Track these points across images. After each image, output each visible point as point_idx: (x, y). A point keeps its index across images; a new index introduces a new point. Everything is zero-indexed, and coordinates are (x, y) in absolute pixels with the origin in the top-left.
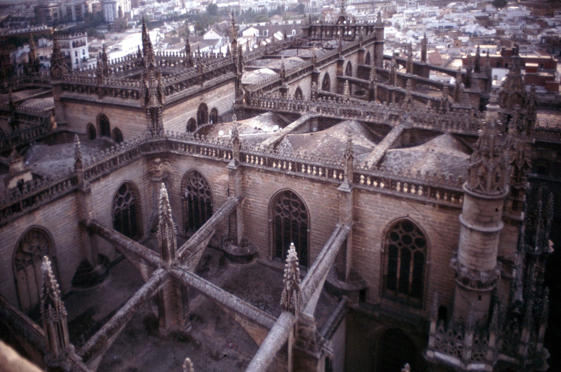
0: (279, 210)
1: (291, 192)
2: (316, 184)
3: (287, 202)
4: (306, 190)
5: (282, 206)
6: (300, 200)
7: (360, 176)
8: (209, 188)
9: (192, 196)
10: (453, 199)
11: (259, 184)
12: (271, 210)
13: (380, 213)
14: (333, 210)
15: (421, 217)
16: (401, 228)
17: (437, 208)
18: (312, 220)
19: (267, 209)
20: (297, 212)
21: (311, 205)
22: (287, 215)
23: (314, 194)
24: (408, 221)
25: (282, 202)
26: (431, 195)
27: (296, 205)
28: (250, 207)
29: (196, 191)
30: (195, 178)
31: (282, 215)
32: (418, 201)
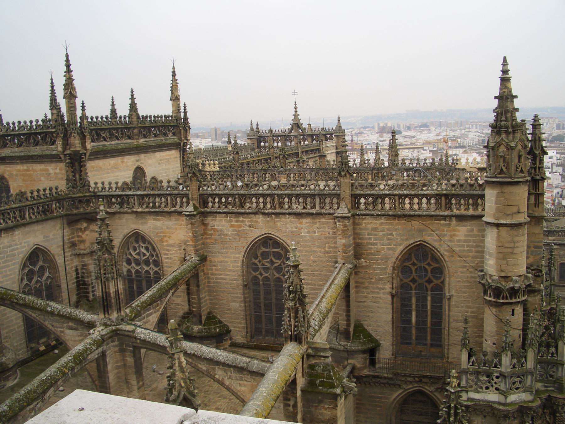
0: (256, 269)
2: (304, 221)
3: (265, 255)
5: (260, 262)
9: (133, 271)
13: (388, 241)
14: (328, 252)
16: (414, 260)
20: (280, 265)
22: (266, 273)
23: (302, 234)
25: (259, 255)
26: (446, 208)
28: (216, 270)
29: (138, 263)
30: (136, 245)
31: (261, 274)
32: (431, 216)
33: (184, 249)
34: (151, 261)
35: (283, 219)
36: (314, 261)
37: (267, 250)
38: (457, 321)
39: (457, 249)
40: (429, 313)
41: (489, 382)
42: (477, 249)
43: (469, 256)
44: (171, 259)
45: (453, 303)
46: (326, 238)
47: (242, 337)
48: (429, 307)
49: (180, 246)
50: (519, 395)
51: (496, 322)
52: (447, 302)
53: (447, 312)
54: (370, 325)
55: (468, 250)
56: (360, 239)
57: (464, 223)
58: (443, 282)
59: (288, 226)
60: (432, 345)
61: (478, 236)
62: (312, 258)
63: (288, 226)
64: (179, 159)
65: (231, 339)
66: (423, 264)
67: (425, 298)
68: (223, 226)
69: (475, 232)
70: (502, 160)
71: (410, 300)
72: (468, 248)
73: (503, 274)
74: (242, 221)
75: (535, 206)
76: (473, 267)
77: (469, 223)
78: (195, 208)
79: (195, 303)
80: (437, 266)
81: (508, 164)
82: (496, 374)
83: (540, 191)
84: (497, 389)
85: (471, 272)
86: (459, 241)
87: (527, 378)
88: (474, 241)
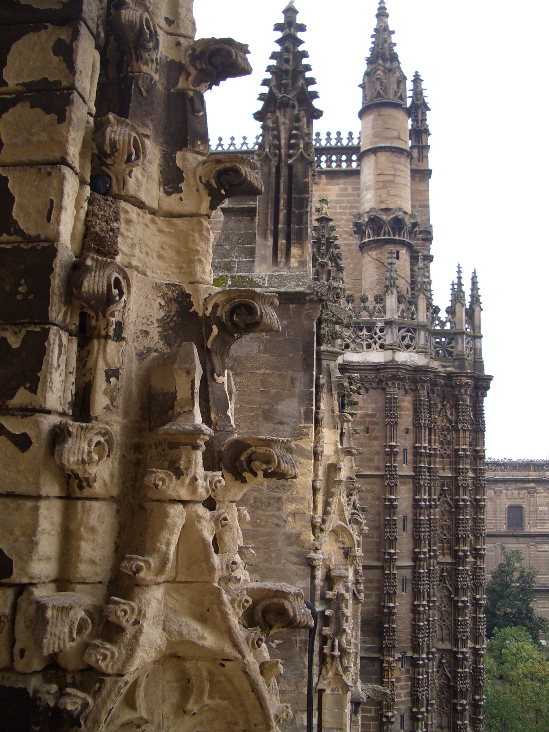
41: (372, 338)
42: (351, 211)
43: (342, 220)
50: (411, 354)
51: (377, 268)
55: (341, 213)
57: (335, 181)
61: (353, 195)
69: (350, 191)
70: (378, 83)
72: (341, 210)
73: (383, 206)
75: (419, 161)
76: (347, 232)
77: (341, 181)
81: (386, 88)
82: (380, 325)
83: (424, 144)
84: (382, 347)
85: (345, 239)
87: (419, 335)
88: (348, 202)
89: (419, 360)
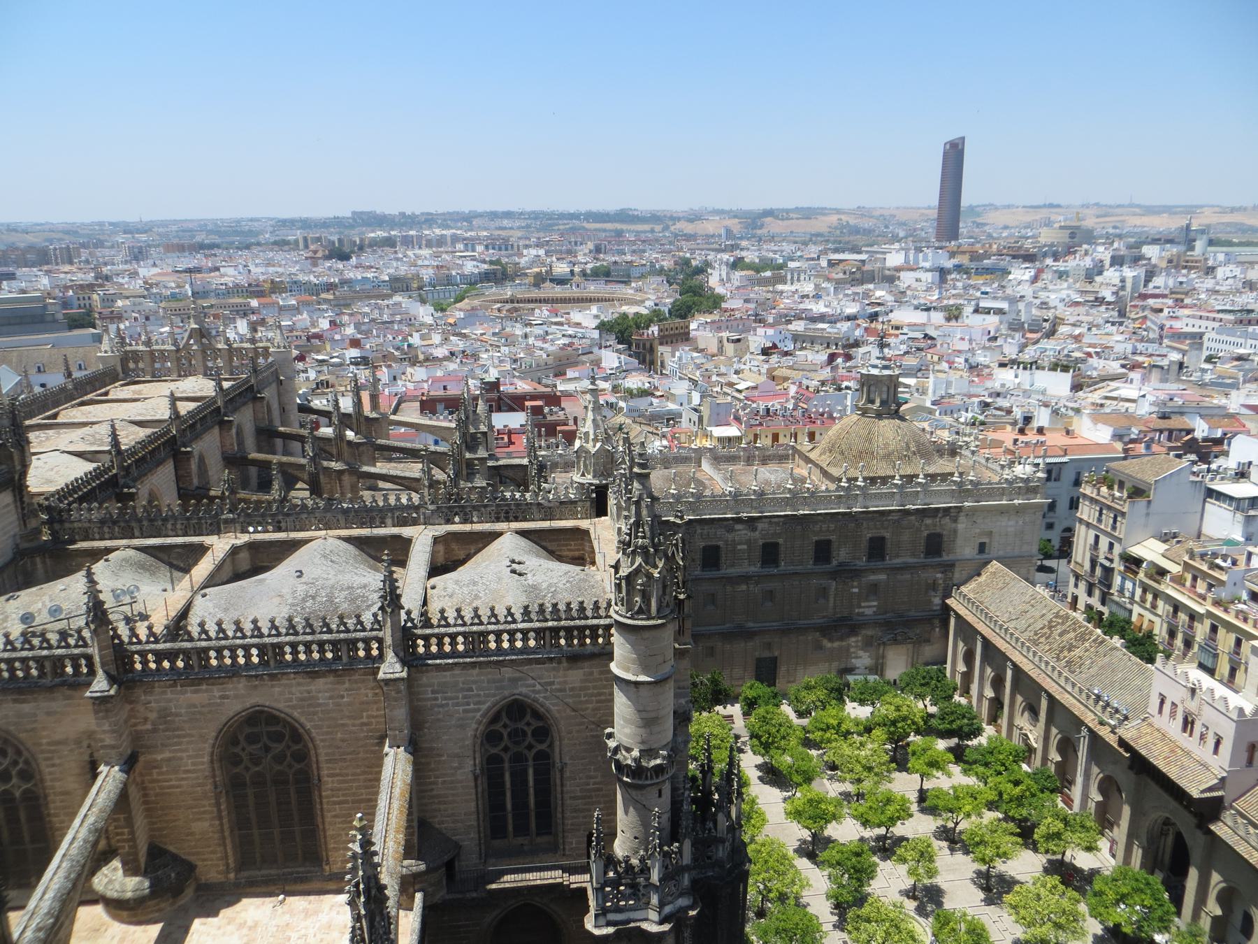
1: (262, 712)
2: (321, 681)
4: (302, 700)
6: (286, 724)
7: (414, 642)
8: (27, 762)
10: (588, 641)
11: (177, 715)
12: (216, 765)
15: (538, 687)
16: (505, 720)
17: (565, 664)
18: (322, 758)
19: (205, 766)
21: (316, 727)
24: (516, 700)
25: (241, 738)
27: (278, 737)
33: (89, 746)
34: (14, 773)
35: (284, 682)
36: (343, 740)
37: (255, 730)
38: (574, 798)
39: (570, 701)
40: (532, 791)
44: (59, 765)
45: (567, 774)
46: (362, 703)
47: (218, 872)
48: (531, 783)
49: (78, 742)
52: (558, 776)
53: (559, 789)
54: (443, 822)
56: (419, 700)
57: (579, 664)
58: (551, 745)
59: (294, 689)
60: (538, 834)
62: (339, 735)
63: (294, 689)
64: (12, 507)
65: (196, 879)
66: (521, 725)
67: (525, 772)
68: (170, 701)
69: (596, 675)
71: (502, 775)
74: (206, 691)
77: (586, 664)
78: (112, 679)
79: (124, 841)
80: (541, 724)
86: (572, 689)
89: (683, 902)
